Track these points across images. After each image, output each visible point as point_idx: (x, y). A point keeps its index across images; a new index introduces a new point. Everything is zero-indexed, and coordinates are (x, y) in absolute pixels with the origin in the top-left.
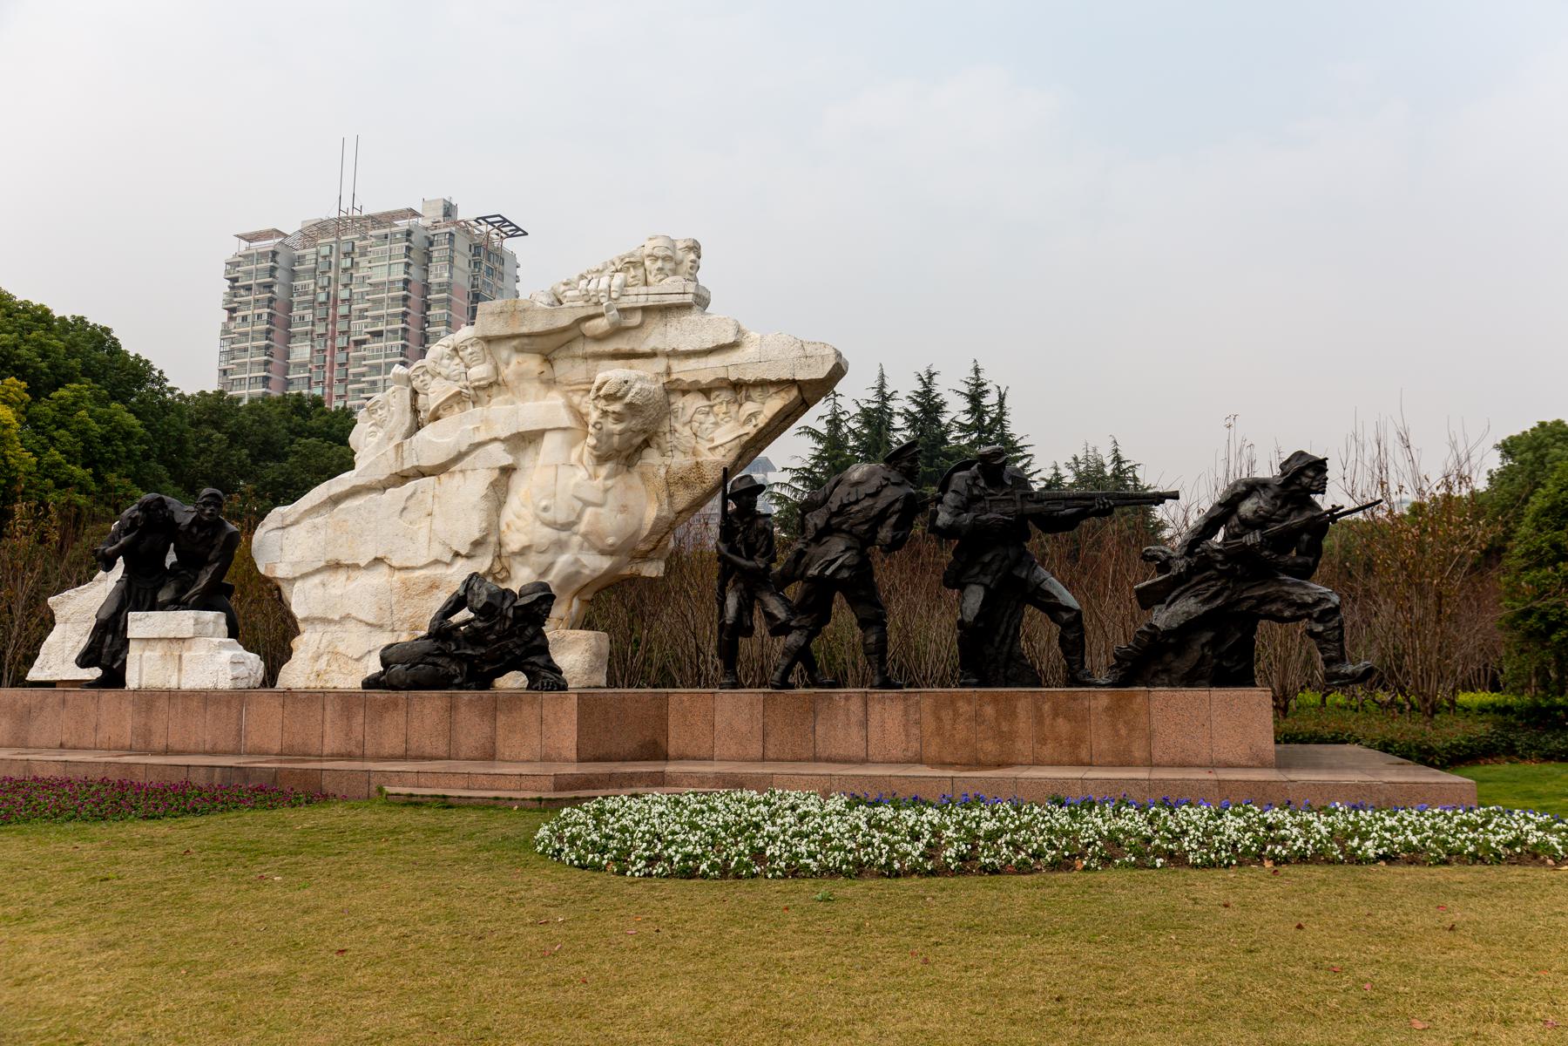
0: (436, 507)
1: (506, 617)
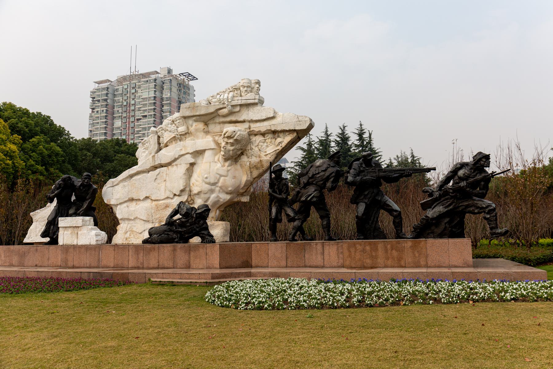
0: (167, 178)
1: (193, 217)
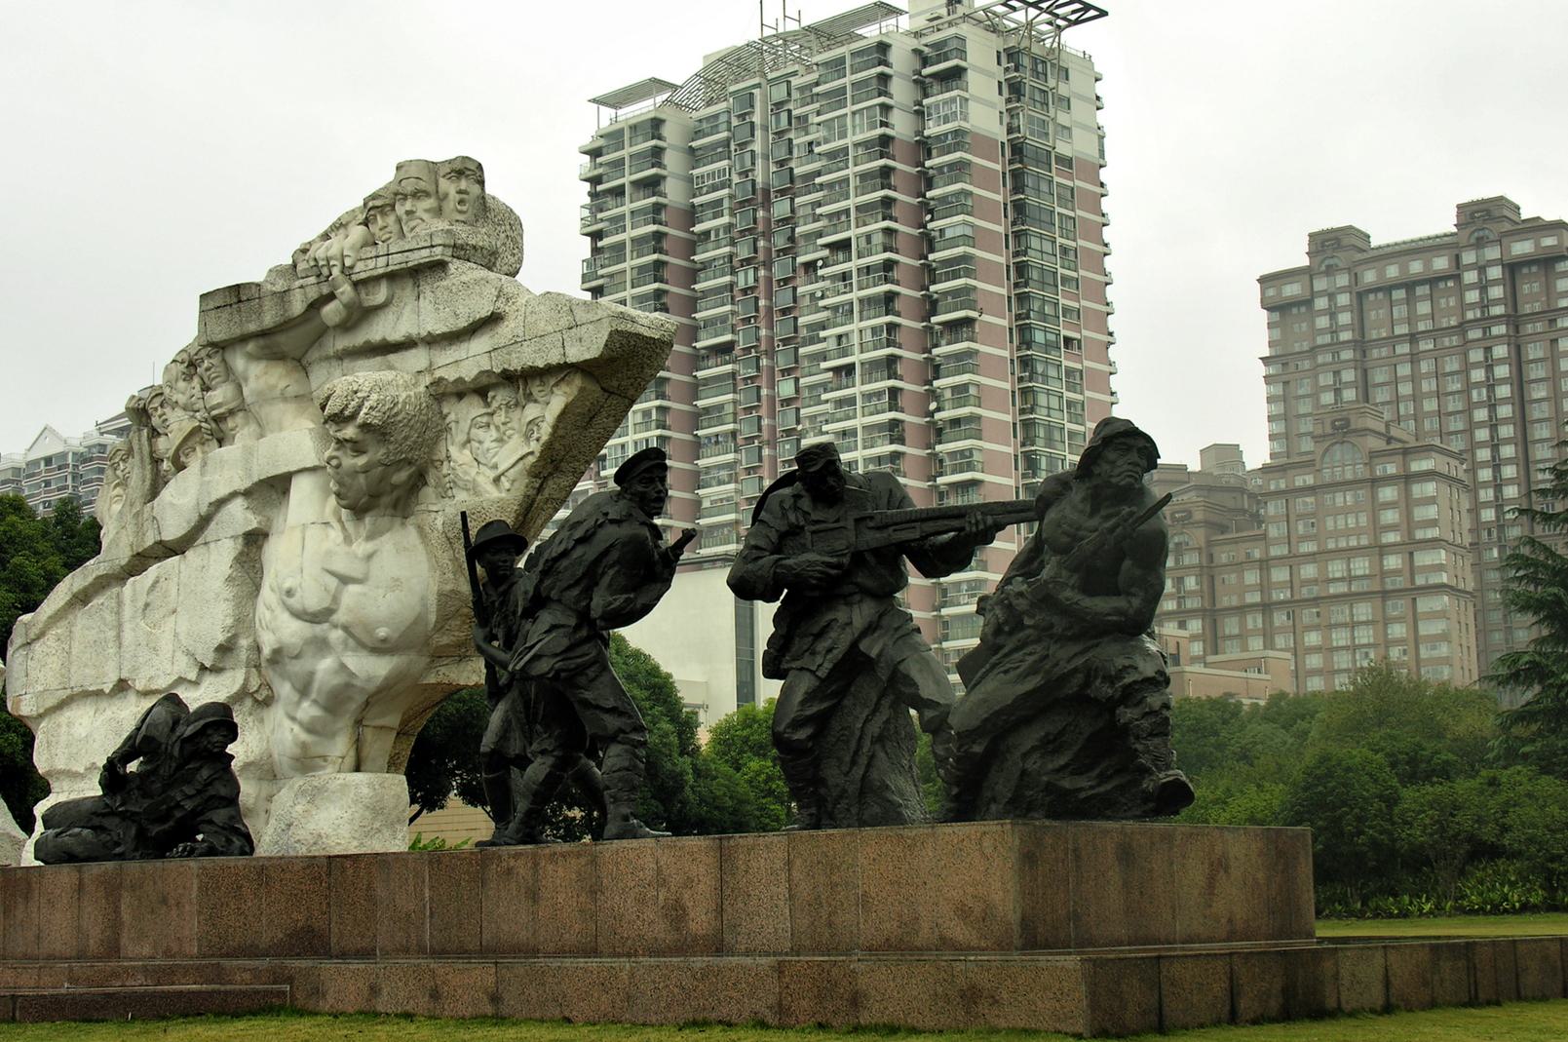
1: (171, 757)
